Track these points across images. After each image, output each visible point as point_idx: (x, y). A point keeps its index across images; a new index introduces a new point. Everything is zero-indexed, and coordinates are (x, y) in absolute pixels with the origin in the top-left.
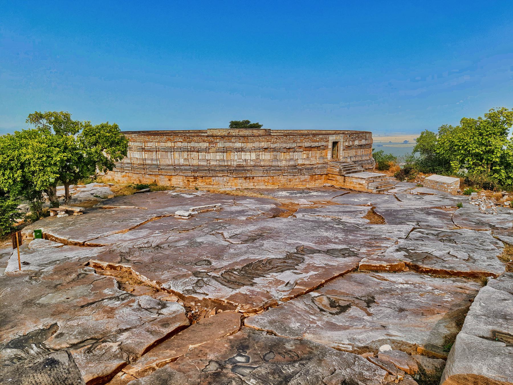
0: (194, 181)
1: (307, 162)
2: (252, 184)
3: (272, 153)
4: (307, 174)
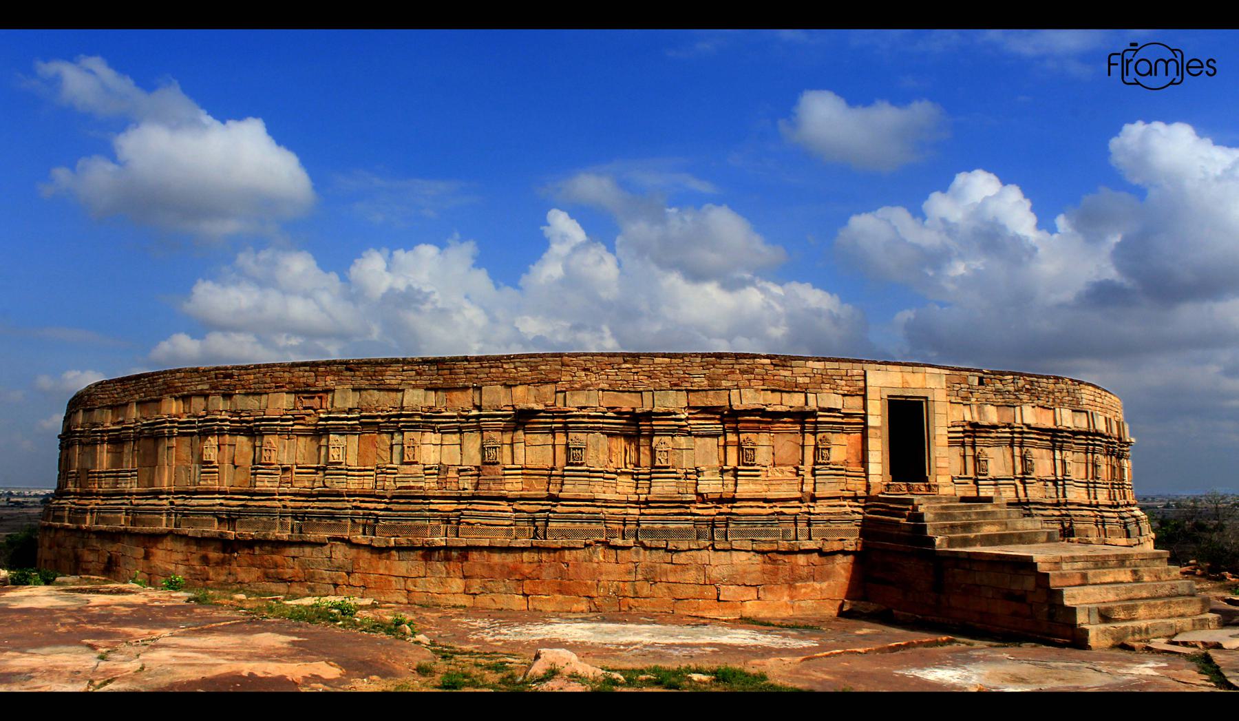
0: (222, 563)
1: (746, 488)
2: (457, 584)
3: (561, 439)
4: (748, 545)
